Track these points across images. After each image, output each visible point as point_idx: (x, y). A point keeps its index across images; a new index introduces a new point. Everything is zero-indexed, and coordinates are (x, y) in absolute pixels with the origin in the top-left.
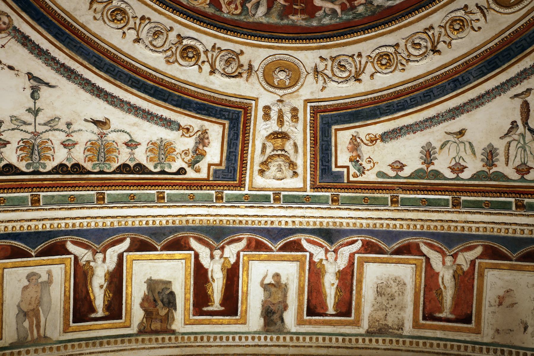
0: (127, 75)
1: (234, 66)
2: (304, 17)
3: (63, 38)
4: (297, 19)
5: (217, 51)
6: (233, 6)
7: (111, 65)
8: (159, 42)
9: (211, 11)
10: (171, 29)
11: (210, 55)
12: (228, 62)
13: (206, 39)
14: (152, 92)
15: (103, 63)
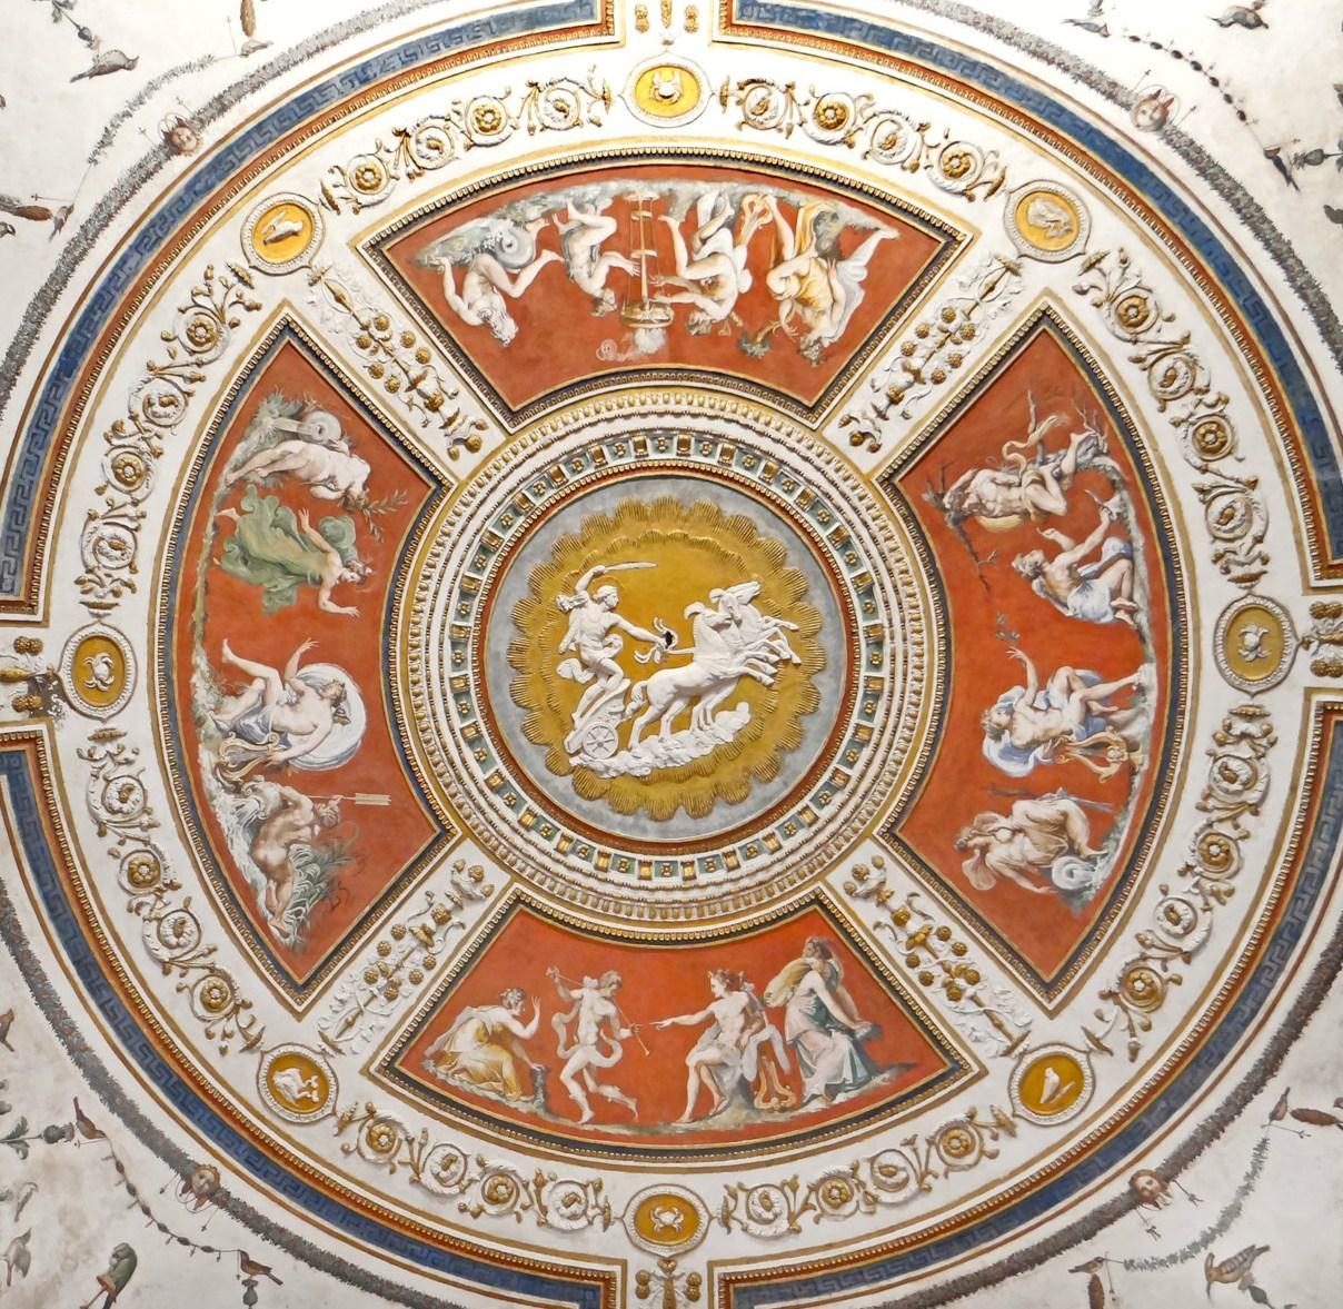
0: (942, 64)
1: (752, 101)
2: (631, 198)
3: (1049, 109)
4: (643, 191)
5: (784, 126)
6: (758, 209)
7: (969, 76)
8: (887, 129)
9: (796, 197)
10: (865, 156)
11: (796, 120)
12: (764, 106)
13: (804, 148)
14: (896, 40)
15: (983, 77)
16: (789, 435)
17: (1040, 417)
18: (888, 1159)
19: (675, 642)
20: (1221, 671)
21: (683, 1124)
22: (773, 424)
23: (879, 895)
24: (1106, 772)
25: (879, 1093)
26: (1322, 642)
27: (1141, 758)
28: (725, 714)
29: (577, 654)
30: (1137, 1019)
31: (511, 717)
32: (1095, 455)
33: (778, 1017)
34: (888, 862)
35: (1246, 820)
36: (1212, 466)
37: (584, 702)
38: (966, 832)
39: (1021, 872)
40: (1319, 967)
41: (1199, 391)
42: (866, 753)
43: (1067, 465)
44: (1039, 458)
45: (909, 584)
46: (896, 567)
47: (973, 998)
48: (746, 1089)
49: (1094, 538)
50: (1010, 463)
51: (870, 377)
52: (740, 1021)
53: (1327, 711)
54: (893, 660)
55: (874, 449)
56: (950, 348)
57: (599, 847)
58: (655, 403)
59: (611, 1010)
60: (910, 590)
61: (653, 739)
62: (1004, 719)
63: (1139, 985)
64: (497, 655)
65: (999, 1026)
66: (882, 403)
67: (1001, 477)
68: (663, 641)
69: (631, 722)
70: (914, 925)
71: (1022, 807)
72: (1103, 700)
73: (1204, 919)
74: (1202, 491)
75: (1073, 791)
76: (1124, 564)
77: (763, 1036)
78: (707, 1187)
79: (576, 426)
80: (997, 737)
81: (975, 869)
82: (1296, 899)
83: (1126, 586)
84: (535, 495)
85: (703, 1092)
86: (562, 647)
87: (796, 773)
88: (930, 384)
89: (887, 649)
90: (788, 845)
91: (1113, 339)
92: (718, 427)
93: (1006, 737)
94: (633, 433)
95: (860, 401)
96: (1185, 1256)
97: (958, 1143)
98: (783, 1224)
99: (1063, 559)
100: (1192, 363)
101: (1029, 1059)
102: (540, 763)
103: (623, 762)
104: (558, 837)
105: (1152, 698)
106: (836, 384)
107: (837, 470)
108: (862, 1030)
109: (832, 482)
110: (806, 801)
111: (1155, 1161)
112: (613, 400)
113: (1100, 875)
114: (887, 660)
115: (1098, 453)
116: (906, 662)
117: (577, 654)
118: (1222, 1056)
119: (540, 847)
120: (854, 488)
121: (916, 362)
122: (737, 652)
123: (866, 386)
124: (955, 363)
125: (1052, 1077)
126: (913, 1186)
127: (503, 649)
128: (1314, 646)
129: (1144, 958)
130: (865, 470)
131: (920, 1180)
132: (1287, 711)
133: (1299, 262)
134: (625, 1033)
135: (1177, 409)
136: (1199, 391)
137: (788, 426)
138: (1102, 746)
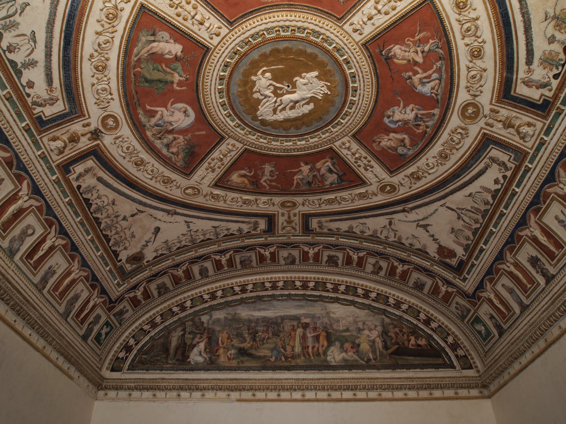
16: (331, 27)
17: (420, 32)
18: (344, 197)
19: (290, 88)
20: (459, 116)
21: (293, 188)
22: (326, 24)
23: (349, 149)
24: (418, 131)
25: (344, 185)
26: (490, 118)
27: (428, 130)
28: (306, 106)
29: (259, 92)
30: (412, 182)
31: (240, 109)
32: (436, 48)
33: (319, 170)
34: (352, 141)
35: (454, 151)
36: (474, 61)
37: (262, 103)
38: (375, 138)
39: (389, 148)
40: (462, 184)
41: (477, 37)
42: (348, 118)
43: (426, 49)
44: (417, 45)
45: (368, 75)
46: (364, 70)
47: (371, 171)
48: (309, 183)
49: (430, 72)
50: (407, 44)
51: (362, 9)
52: (308, 171)
53: (485, 134)
54: (360, 95)
55: (361, 34)
56: (392, 3)
57: (268, 137)
58: (282, 16)
59: (273, 169)
60: (368, 77)
61: (283, 112)
62: (391, 114)
63: (415, 176)
64: (234, 94)
65: (377, 177)
66: (365, 19)
67: (403, 48)
68: (286, 88)
69: (277, 108)
70: (357, 156)
71: (392, 135)
72: (421, 114)
73: (436, 168)
74: (468, 68)
75: (406, 134)
76: (437, 81)
77: (314, 174)
78: (299, 199)
79: (254, 25)
80: (389, 117)
81: (376, 146)
82: (461, 170)
83: (436, 88)
84: (242, 48)
85: (298, 183)
86: (254, 90)
87: (327, 120)
88: (383, 15)
89: (358, 92)
90: (323, 136)
91: (452, 12)
92: (306, 25)
93: (391, 118)
94: (275, 27)
95: (357, 18)
96: (412, 222)
97: (362, 196)
98: (318, 206)
99: (418, 76)
100: (477, 28)
101: (383, 184)
102: (250, 119)
103: (275, 117)
104: (256, 136)
105: (437, 117)
106: (349, 12)
107: (347, 40)
108: (340, 174)
109: (345, 44)
110: (330, 127)
111: (410, 206)
112: (267, 16)
113: (410, 153)
114: (358, 96)
115: (438, 47)
116: (363, 97)
117: (259, 92)
118: (432, 193)
119: (252, 138)
120: (352, 46)
121: (379, 7)
122: (310, 91)
123: (360, 12)
124: (394, 9)
125: (388, 188)
126: (350, 201)
127: (235, 92)
128: (487, 118)
129: (418, 171)
130: (357, 40)
131: (352, 201)
132: (474, 130)
133: (526, 4)
134: (277, 173)
135: (467, 40)
136: (477, 37)
137: (331, 24)
138: (420, 125)
